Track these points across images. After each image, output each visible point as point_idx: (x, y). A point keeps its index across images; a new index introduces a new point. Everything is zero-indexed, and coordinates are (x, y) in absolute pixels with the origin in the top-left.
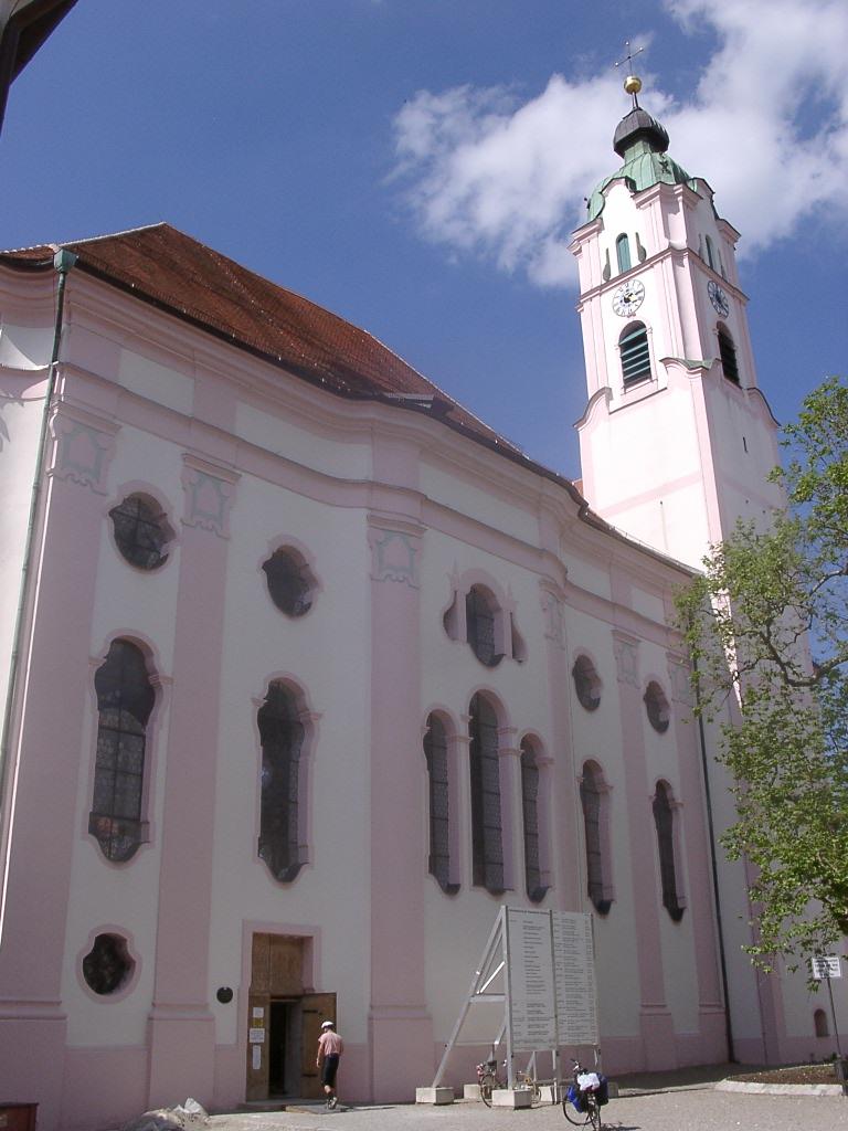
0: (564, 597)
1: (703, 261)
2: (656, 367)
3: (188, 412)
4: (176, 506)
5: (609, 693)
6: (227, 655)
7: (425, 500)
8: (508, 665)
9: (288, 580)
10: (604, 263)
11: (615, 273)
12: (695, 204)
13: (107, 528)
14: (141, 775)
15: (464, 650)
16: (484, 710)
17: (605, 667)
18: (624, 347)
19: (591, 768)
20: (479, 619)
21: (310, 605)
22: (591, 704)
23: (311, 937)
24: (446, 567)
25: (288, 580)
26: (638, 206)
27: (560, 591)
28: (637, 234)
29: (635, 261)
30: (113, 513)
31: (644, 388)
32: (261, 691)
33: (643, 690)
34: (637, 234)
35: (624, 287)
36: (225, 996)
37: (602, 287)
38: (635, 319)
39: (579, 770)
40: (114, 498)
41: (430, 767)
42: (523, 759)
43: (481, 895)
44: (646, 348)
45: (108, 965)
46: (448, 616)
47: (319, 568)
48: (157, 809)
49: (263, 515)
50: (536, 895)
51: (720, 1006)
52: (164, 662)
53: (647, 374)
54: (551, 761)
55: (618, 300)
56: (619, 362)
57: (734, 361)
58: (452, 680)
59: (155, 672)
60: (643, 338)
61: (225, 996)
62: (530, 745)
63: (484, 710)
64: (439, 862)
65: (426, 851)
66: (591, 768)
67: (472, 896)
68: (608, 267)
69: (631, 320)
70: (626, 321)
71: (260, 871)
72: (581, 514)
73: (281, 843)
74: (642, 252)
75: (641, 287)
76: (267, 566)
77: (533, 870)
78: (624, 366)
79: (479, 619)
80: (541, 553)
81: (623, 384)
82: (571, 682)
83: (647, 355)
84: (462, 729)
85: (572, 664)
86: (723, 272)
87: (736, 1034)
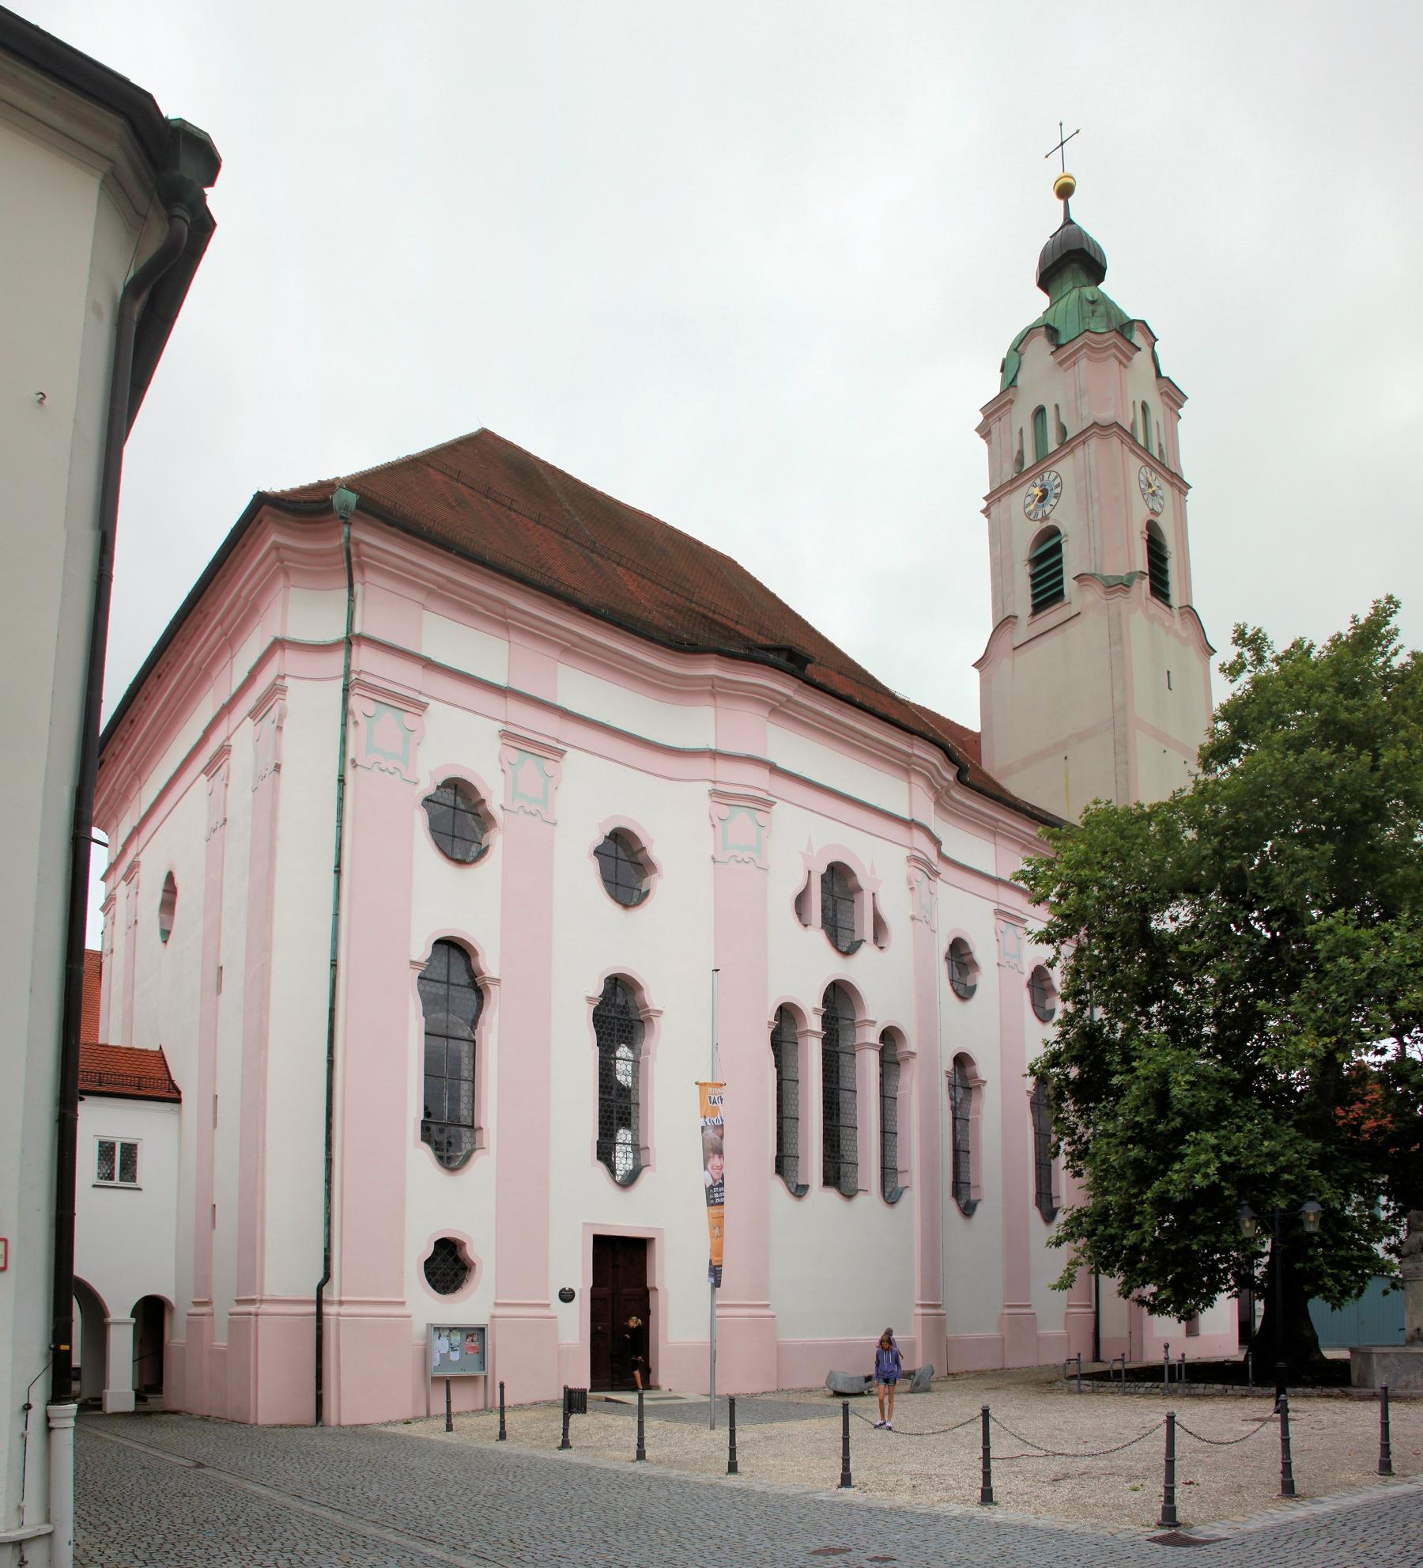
0: (937, 874)
2: (1069, 585)
3: (501, 680)
4: (494, 794)
5: (987, 979)
6: (554, 945)
7: (773, 768)
8: (867, 951)
9: (624, 864)
10: (1016, 448)
12: (1129, 359)
13: (420, 820)
14: (473, 1082)
15: (817, 937)
16: (839, 999)
17: (983, 952)
18: (1036, 561)
19: (962, 1061)
20: (836, 899)
21: (647, 893)
22: (965, 993)
23: (653, 1239)
24: (801, 840)
25: (624, 864)
26: (1061, 363)
27: (934, 864)
28: (1057, 406)
29: (1052, 446)
30: (428, 801)
32: (596, 989)
33: (1028, 975)
34: (1057, 406)
35: (1038, 482)
36: (567, 1296)
38: (1050, 523)
39: (948, 1065)
40: (427, 785)
41: (778, 1065)
42: (882, 1052)
43: (832, 1194)
44: (1060, 561)
45: (448, 1266)
46: (801, 901)
47: (656, 852)
48: (490, 1112)
49: (596, 793)
50: (891, 1195)
51: (1089, 1306)
52: (489, 963)
53: (1059, 595)
54: (913, 1054)
56: (1028, 582)
57: (1165, 572)
58: (804, 967)
59: (482, 973)
60: (1057, 548)
61: (567, 1296)
63: (839, 999)
64: (784, 1163)
65: (772, 1151)
66: (962, 1061)
68: (1021, 453)
69: (1045, 525)
70: (1036, 528)
72: (960, 778)
74: (1063, 430)
75: (1058, 481)
76: (597, 852)
77: (888, 1170)
78: (1034, 586)
79: (836, 899)
80: (910, 824)
81: (1030, 610)
82: (942, 969)
83: (1060, 571)
84: (814, 1023)
86: (1161, 452)
87: (1103, 1335)
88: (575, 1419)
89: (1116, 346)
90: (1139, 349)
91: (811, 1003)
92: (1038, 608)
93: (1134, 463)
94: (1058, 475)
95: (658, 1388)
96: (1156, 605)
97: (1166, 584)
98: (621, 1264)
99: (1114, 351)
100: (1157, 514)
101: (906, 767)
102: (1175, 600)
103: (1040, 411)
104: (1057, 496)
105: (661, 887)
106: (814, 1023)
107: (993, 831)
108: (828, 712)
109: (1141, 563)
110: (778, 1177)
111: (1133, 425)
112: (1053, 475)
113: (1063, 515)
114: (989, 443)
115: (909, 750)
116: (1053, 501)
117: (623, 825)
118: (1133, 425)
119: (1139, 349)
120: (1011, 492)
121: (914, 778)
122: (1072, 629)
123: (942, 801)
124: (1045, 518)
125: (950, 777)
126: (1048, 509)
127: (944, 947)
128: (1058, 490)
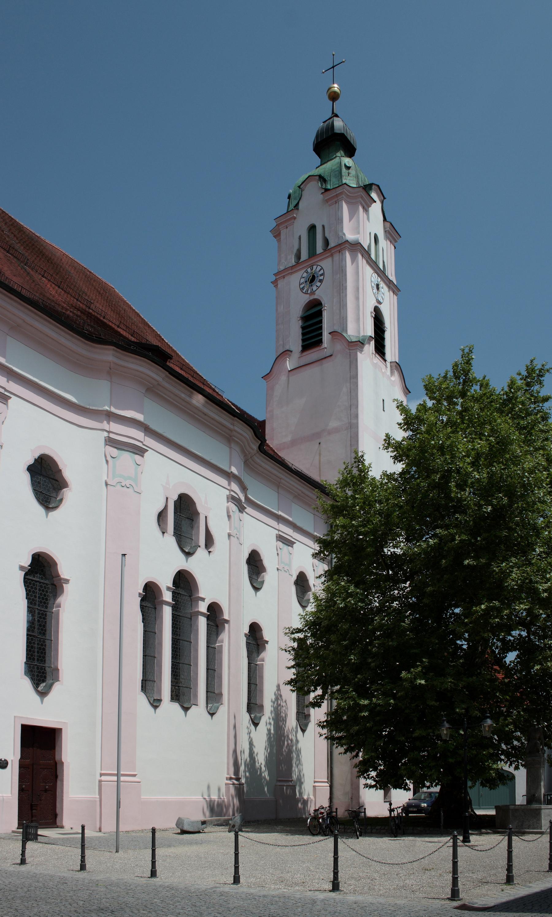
1: (369, 255)
2: (326, 336)
5: (270, 577)
8: (201, 552)
11: (304, 255)
15: (170, 540)
16: (184, 582)
17: (269, 560)
18: (305, 319)
19: (255, 630)
20: (184, 516)
21: (61, 500)
26: (327, 201)
28: (323, 226)
31: (313, 354)
33: (294, 577)
34: (323, 226)
37: (292, 267)
38: (315, 297)
39: (246, 630)
43: (176, 706)
46: (161, 516)
47: (68, 474)
53: (320, 342)
55: (303, 280)
56: (300, 331)
57: (383, 339)
58: (161, 561)
62: (214, 610)
63: (184, 582)
66: (255, 630)
67: (169, 707)
69: (312, 297)
71: (27, 683)
73: (40, 666)
74: (326, 242)
75: (322, 272)
79: (184, 516)
81: (300, 348)
85: (246, 556)
88: (30, 845)
89: (362, 197)
90: (375, 202)
91: (165, 582)
92: (306, 347)
93: (368, 271)
94: (322, 268)
95: (62, 827)
96: (377, 359)
97: (383, 346)
98: (40, 745)
99: (360, 199)
100: (380, 303)
101: (228, 438)
103: (312, 229)
104: (321, 281)
105: (70, 496)
106: (168, 596)
107: (277, 485)
108: (183, 395)
109: (369, 330)
110: (143, 693)
111: (369, 247)
112: (319, 268)
114: (279, 241)
115: (231, 427)
116: (318, 284)
117: (47, 452)
118: (369, 247)
119: (375, 202)
120: (292, 273)
121: (233, 445)
122: (328, 365)
123: (248, 464)
124: (313, 293)
125: (255, 447)
126: (315, 288)
127: (246, 555)
128: (321, 278)
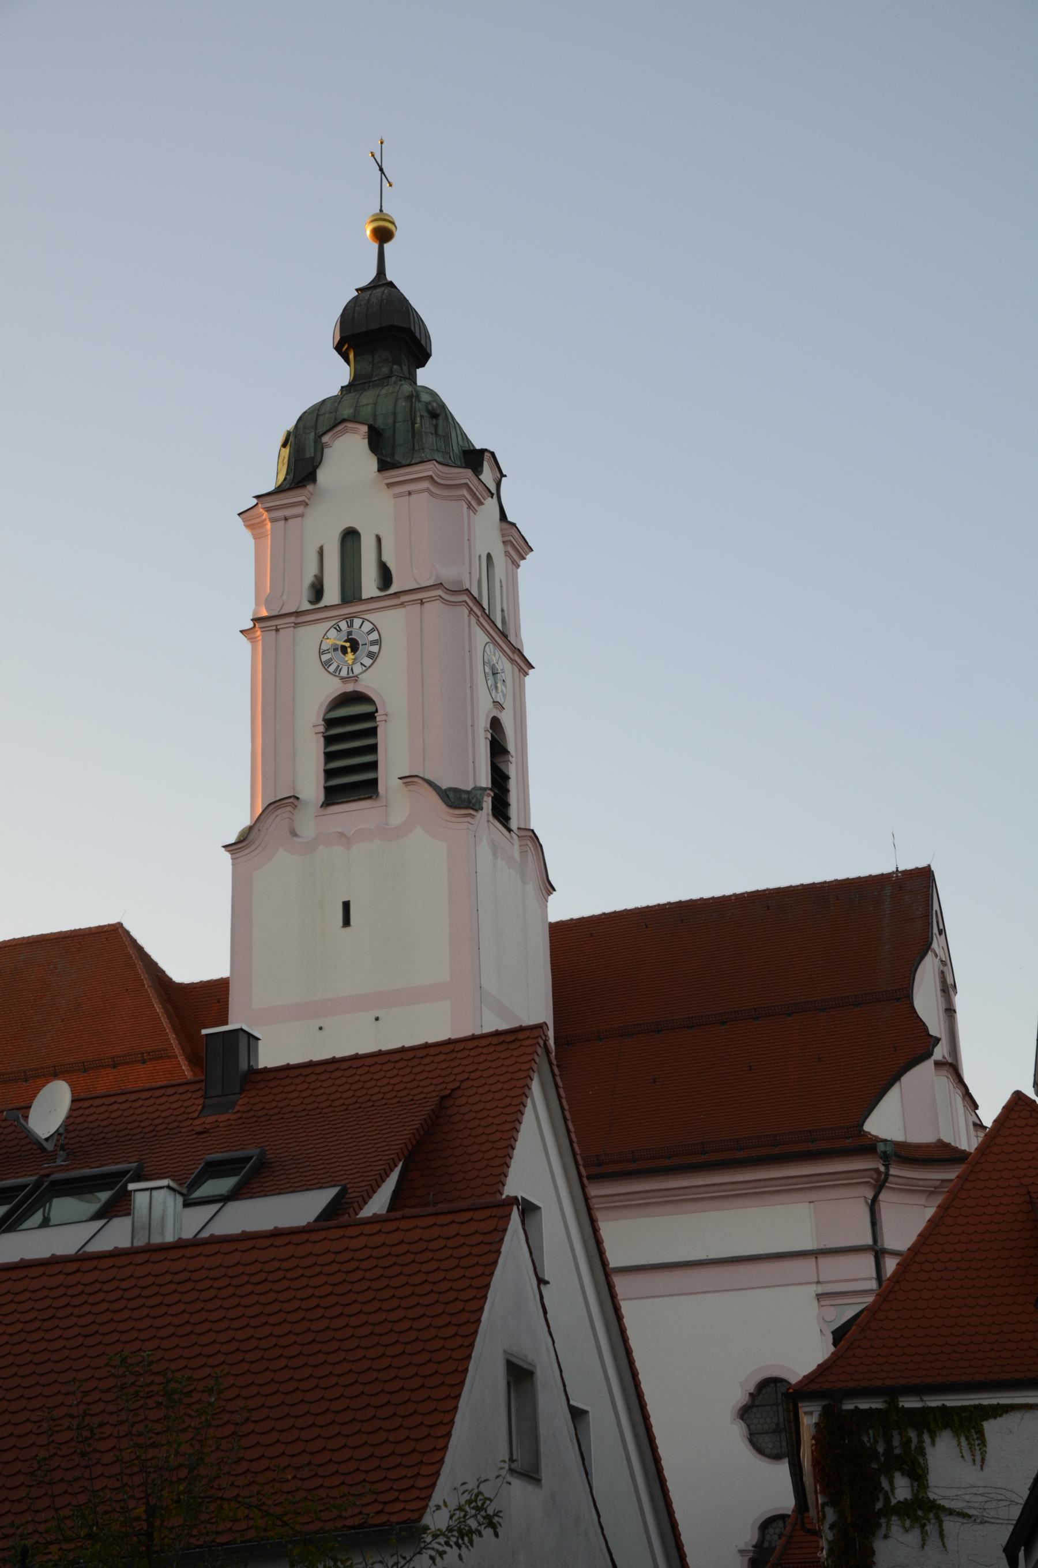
11: (332, 594)
28: (379, 539)
29: (369, 586)
31: (353, 814)
34: (379, 539)
38: (359, 688)
53: (369, 789)
57: (506, 791)
69: (350, 688)
75: (374, 636)
81: (321, 797)
92: (334, 795)
97: (507, 805)
102: (514, 824)
103: (350, 537)
104: (372, 656)
112: (367, 626)
113: (386, 681)
128: (375, 649)
